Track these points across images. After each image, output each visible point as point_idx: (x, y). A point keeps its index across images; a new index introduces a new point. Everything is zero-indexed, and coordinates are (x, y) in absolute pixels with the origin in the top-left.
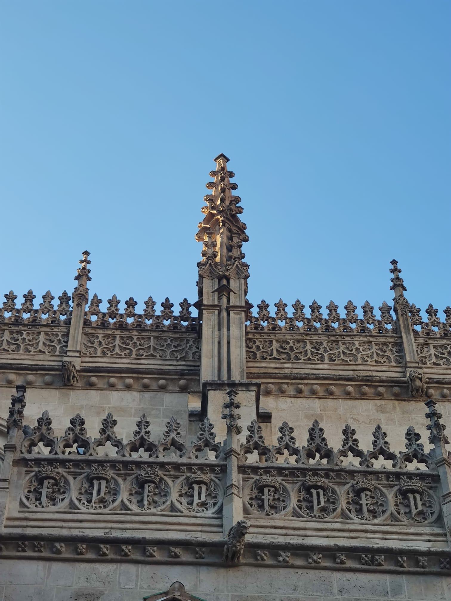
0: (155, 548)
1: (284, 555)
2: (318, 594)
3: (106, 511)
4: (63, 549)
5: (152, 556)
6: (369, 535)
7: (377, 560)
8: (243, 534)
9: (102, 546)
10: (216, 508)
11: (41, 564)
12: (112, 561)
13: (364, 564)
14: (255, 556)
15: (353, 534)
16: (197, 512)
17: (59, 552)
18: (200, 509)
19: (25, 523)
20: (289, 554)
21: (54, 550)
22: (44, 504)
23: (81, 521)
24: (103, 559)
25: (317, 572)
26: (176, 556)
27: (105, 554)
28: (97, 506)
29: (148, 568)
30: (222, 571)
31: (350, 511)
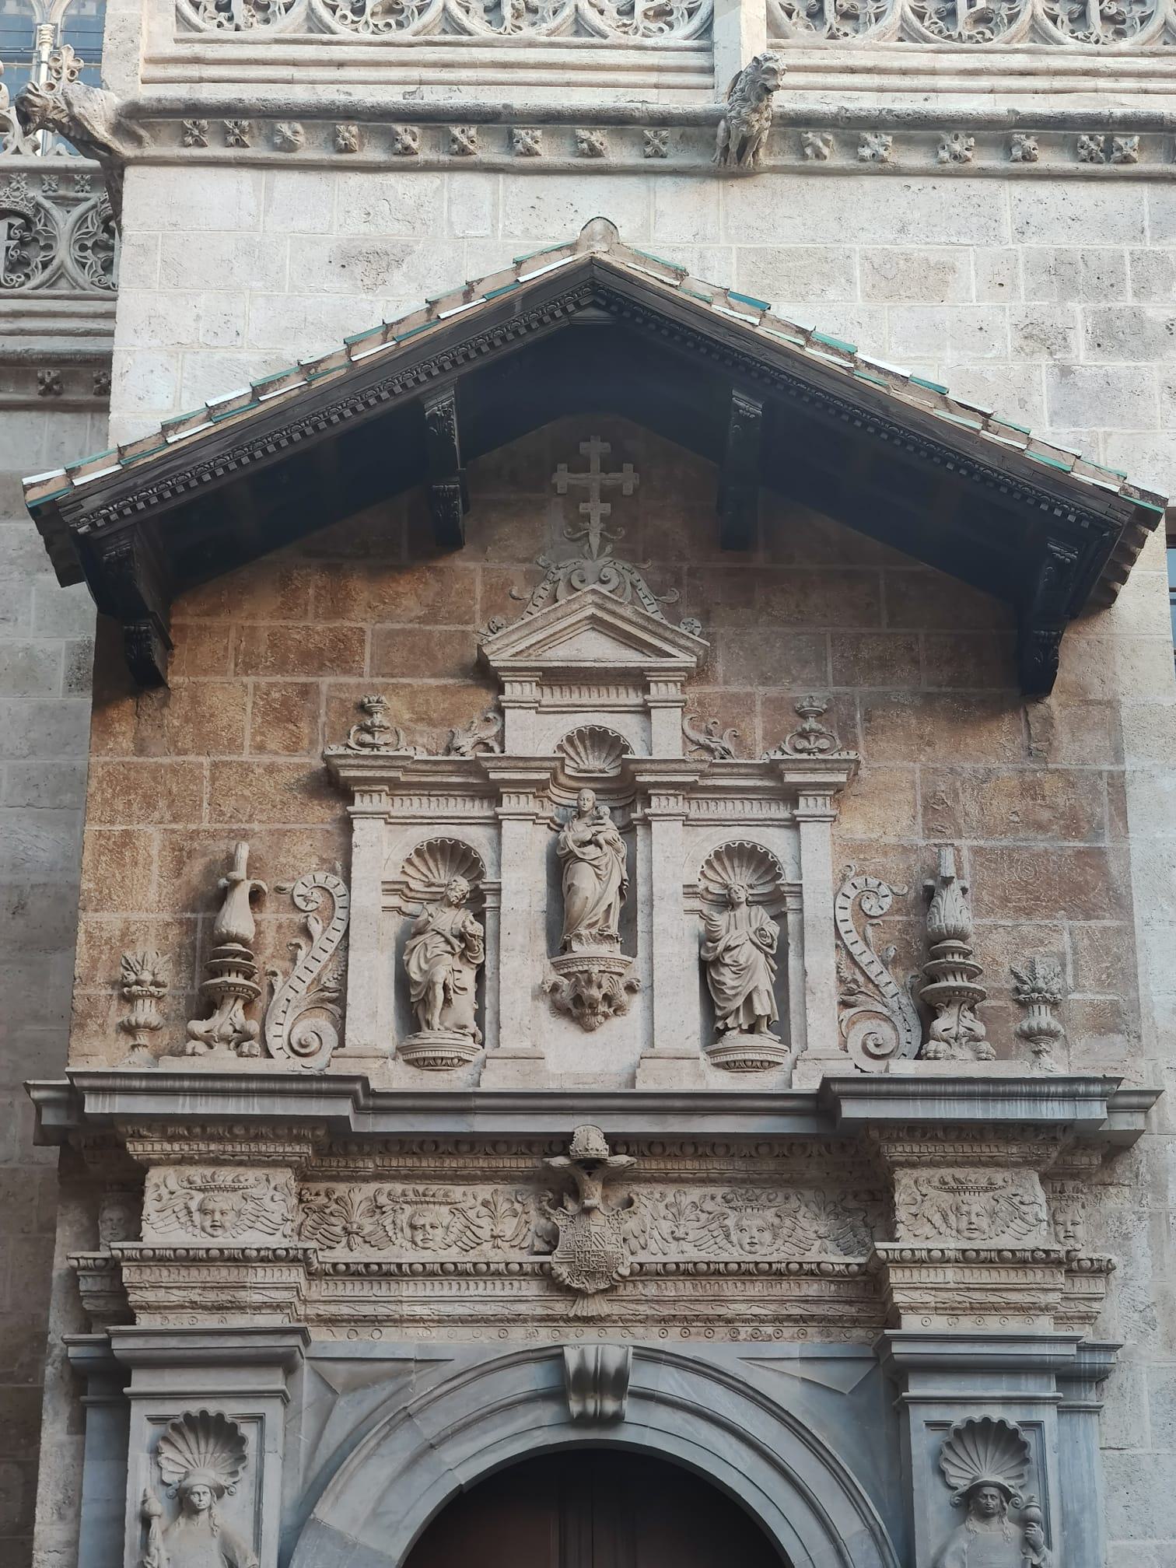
0: (538, 133)
1: (875, 143)
2: (963, 240)
3: (405, 35)
4: (301, 139)
5: (530, 152)
6: (1102, 83)
7: (1120, 149)
8: (769, 91)
9: (399, 128)
10: (696, 21)
11: (247, 176)
12: (428, 167)
13: (1084, 161)
14: (800, 148)
15: (1059, 83)
16: (644, 35)
17: (289, 146)
18: (654, 26)
19: (194, 71)
20: (890, 139)
21: (278, 140)
22: (239, 19)
23: (341, 64)
24: (404, 163)
25: (961, 183)
26: (593, 152)
27: (407, 150)
28: (381, 24)
29: (523, 181)
30: (713, 188)
31: (1054, 19)
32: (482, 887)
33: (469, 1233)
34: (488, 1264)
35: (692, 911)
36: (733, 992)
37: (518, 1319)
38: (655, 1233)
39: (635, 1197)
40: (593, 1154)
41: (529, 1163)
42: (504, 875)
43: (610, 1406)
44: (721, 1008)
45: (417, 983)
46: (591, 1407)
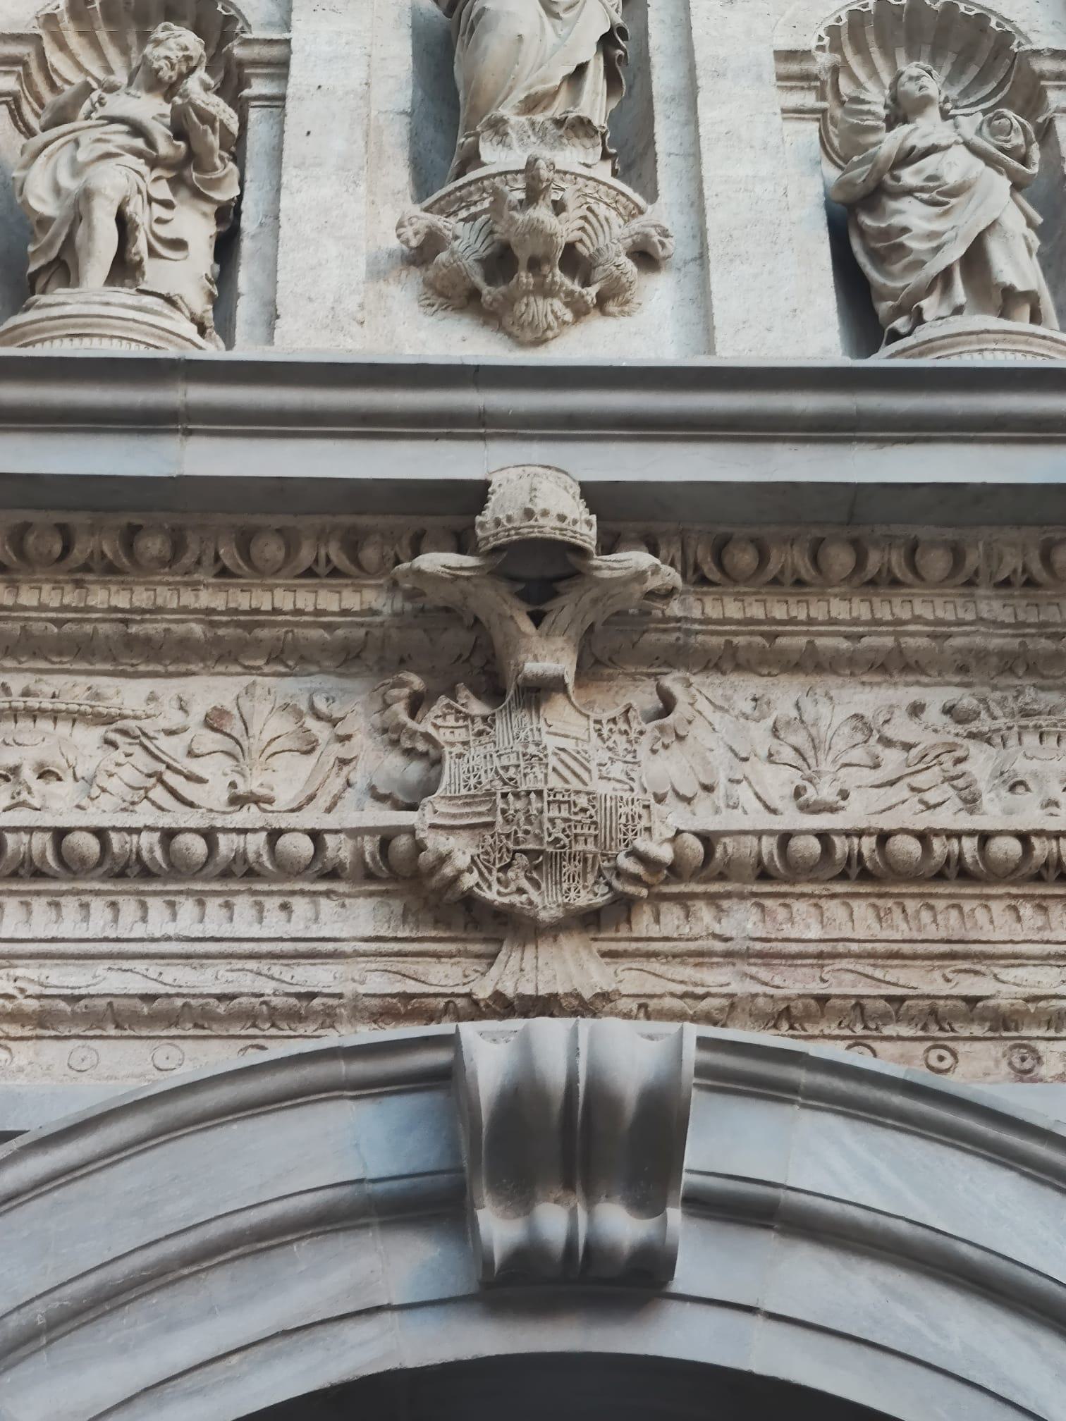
32: (239, 52)
33: (159, 794)
34: (209, 835)
35: (799, 112)
36: (934, 244)
37: (303, 1009)
38: (744, 793)
39: (677, 690)
40: (548, 528)
41: (352, 600)
42: (295, 24)
43: (621, 1225)
44: (893, 295)
45: (44, 222)
46: (554, 1221)
